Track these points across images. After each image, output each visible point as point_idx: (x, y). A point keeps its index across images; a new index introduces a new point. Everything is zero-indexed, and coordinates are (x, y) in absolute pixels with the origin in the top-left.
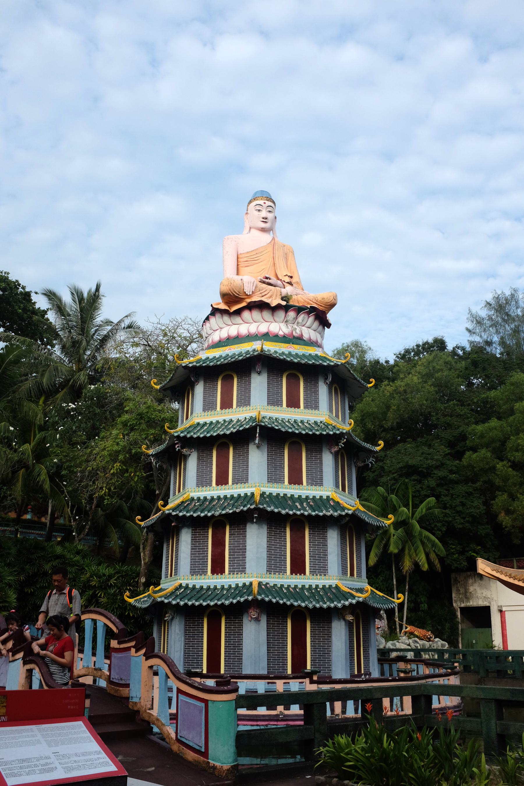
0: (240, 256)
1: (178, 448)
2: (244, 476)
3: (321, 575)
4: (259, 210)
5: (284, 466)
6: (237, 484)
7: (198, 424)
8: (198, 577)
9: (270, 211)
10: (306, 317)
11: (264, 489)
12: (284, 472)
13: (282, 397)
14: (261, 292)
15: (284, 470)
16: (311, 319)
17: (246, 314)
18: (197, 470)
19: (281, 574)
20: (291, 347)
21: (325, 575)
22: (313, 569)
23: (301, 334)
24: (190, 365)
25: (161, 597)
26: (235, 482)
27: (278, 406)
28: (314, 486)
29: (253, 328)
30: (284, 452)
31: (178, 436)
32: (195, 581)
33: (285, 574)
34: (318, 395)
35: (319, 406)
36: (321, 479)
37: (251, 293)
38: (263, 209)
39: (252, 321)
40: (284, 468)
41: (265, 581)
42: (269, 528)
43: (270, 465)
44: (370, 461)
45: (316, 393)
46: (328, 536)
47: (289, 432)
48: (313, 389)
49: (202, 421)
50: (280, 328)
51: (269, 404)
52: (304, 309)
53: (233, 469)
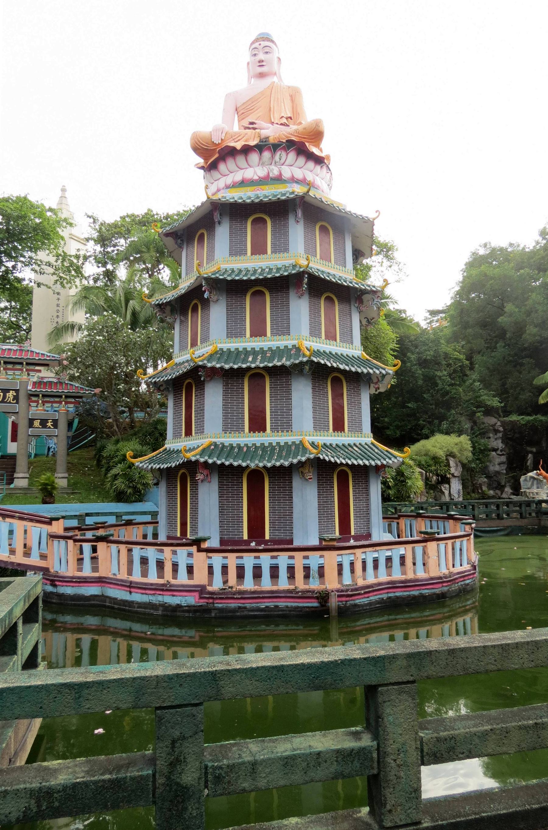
0: (238, 111)
3: (282, 431)
4: (255, 55)
5: (245, 319)
9: (267, 53)
10: (284, 154)
11: (220, 346)
14: (234, 138)
16: (292, 155)
17: (222, 167)
19: (228, 433)
20: (258, 190)
21: (288, 431)
22: (275, 426)
23: (278, 173)
32: (174, 445)
33: (242, 432)
36: (288, 328)
37: (220, 142)
38: (259, 52)
41: (219, 441)
42: (226, 385)
45: (286, 234)
46: (293, 388)
50: (255, 173)
51: (231, 254)
52: (279, 145)
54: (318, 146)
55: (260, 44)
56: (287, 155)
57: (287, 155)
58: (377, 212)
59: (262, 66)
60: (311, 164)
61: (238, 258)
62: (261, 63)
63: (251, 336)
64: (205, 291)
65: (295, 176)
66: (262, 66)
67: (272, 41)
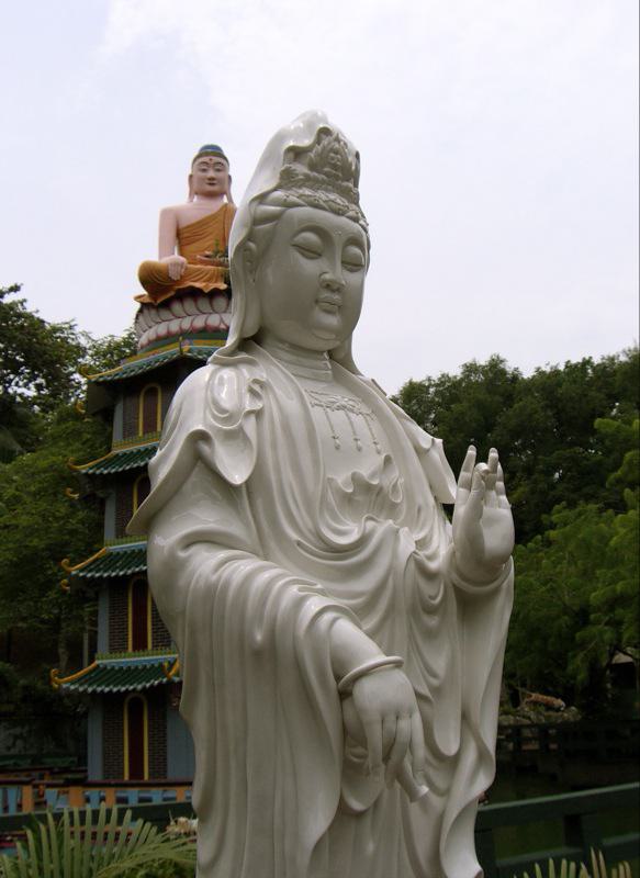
8: (118, 655)
9: (218, 170)
17: (177, 307)
24: (101, 379)
25: (66, 682)
29: (186, 324)
31: (86, 474)
50: (222, 321)
62: (212, 182)
67: (225, 158)
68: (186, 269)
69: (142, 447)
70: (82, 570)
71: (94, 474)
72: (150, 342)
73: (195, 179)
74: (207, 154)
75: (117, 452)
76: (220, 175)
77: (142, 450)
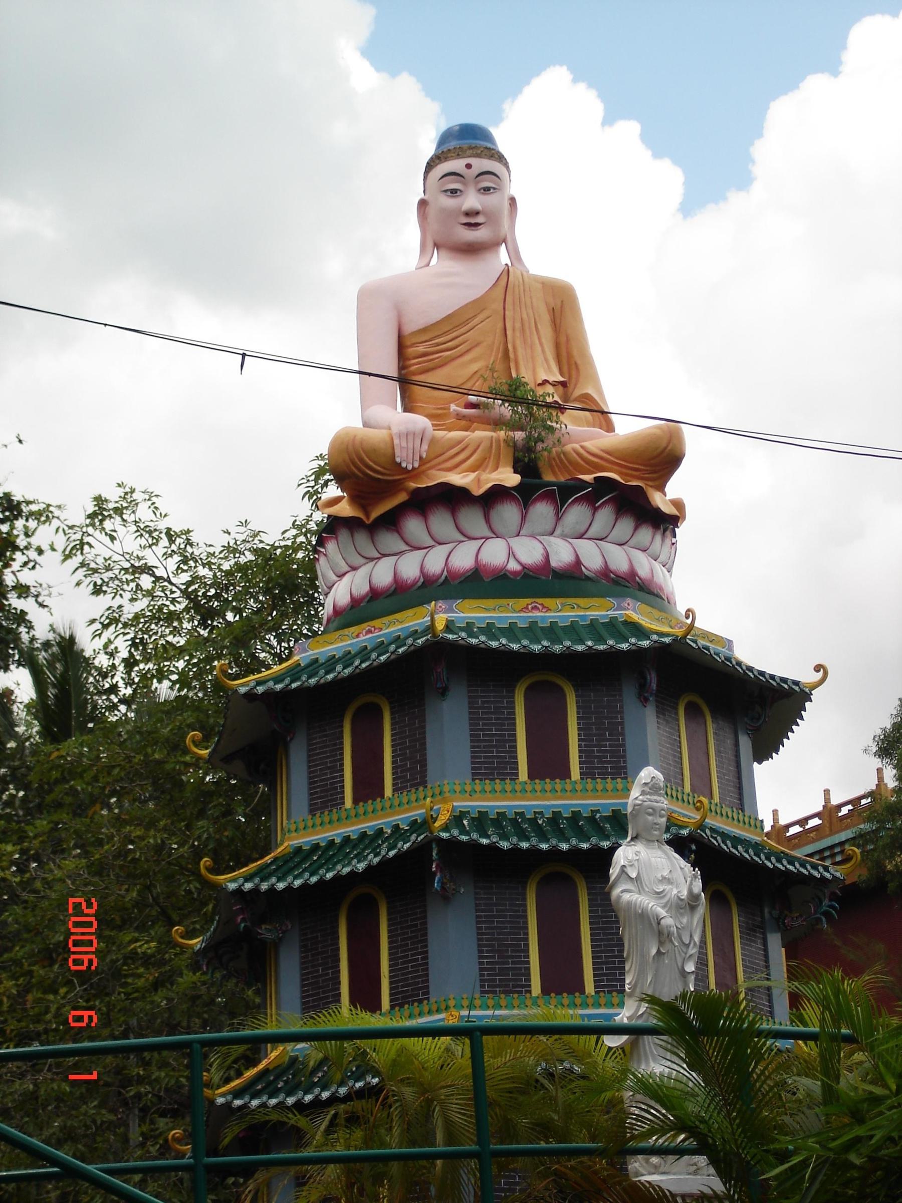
1: (243, 925)
2: (418, 983)
4: (454, 192)
5: (527, 945)
6: (401, 1006)
7: (299, 850)
9: (487, 190)
12: (528, 963)
13: (516, 752)
15: (528, 957)
16: (605, 514)
17: (413, 526)
18: (303, 980)
20: (535, 608)
24: (260, 689)
26: (398, 1002)
27: (504, 780)
28: (614, 994)
29: (435, 562)
30: (525, 906)
31: (239, 891)
34: (623, 734)
35: (625, 767)
37: (416, 465)
39: (432, 543)
40: (527, 951)
43: (485, 946)
44: (825, 908)
45: (617, 730)
47: (521, 850)
48: (606, 718)
49: (304, 840)
50: (511, 553)
53: (390, 966)
54: (661, 488)
55: (469, 166)
56: (594, 514)
57: (594, 514)
58: (818, 668)
59: (477, 225)
60: (645, 534)
61: (498, 785)
62: (471, 219)
63: (546, 991)
64: (435, 874)
65: (613, 566)
66: (477, 225)
67: (501, 158)
68: (433, 441)
69: (352, 829)
70: (237, 1093)
71: (256, 890)
72: (355, 602)
73: (431, 211)
74: (459, 153)
75: (296, 842)
76: (491, 200)
77: (354, 837)
